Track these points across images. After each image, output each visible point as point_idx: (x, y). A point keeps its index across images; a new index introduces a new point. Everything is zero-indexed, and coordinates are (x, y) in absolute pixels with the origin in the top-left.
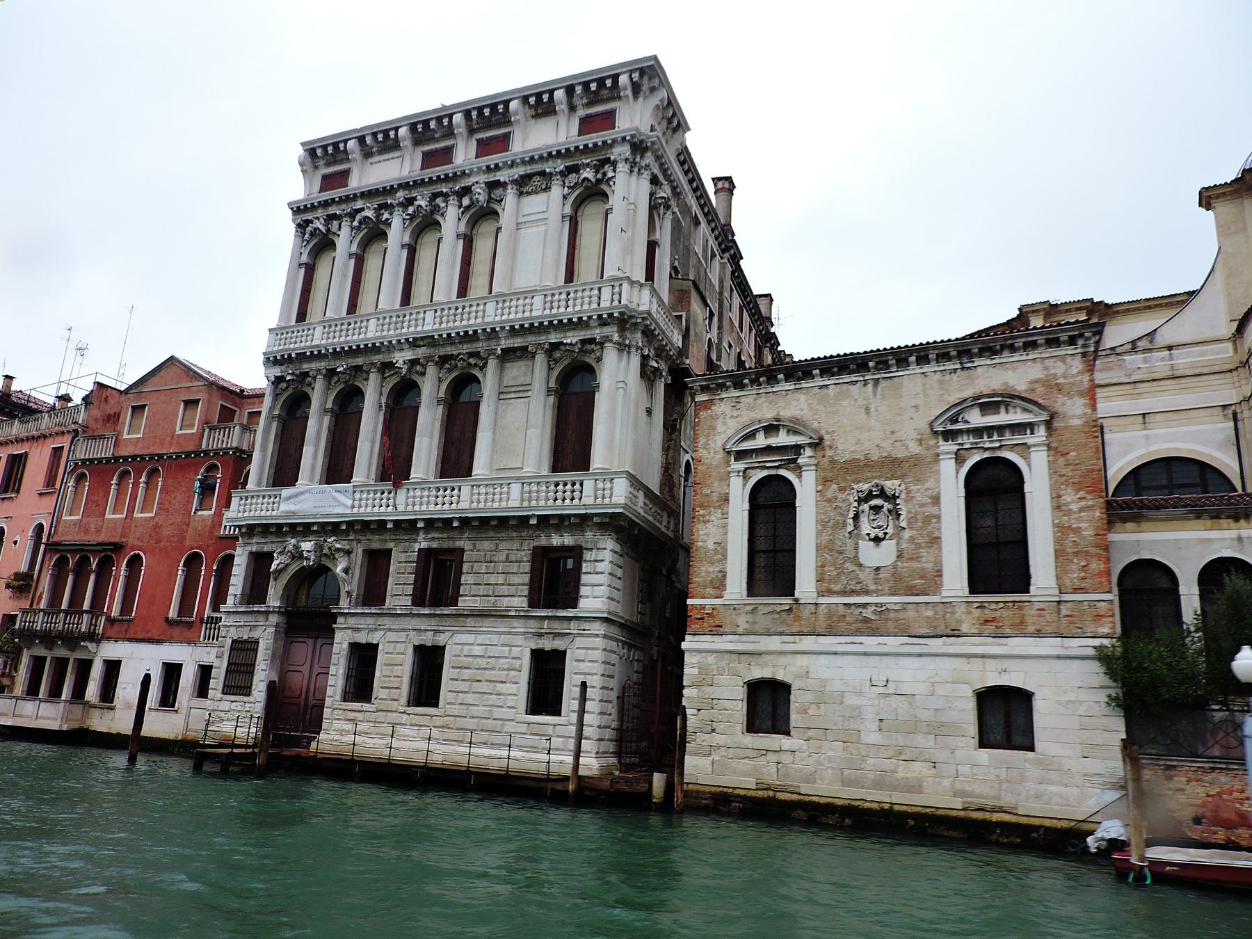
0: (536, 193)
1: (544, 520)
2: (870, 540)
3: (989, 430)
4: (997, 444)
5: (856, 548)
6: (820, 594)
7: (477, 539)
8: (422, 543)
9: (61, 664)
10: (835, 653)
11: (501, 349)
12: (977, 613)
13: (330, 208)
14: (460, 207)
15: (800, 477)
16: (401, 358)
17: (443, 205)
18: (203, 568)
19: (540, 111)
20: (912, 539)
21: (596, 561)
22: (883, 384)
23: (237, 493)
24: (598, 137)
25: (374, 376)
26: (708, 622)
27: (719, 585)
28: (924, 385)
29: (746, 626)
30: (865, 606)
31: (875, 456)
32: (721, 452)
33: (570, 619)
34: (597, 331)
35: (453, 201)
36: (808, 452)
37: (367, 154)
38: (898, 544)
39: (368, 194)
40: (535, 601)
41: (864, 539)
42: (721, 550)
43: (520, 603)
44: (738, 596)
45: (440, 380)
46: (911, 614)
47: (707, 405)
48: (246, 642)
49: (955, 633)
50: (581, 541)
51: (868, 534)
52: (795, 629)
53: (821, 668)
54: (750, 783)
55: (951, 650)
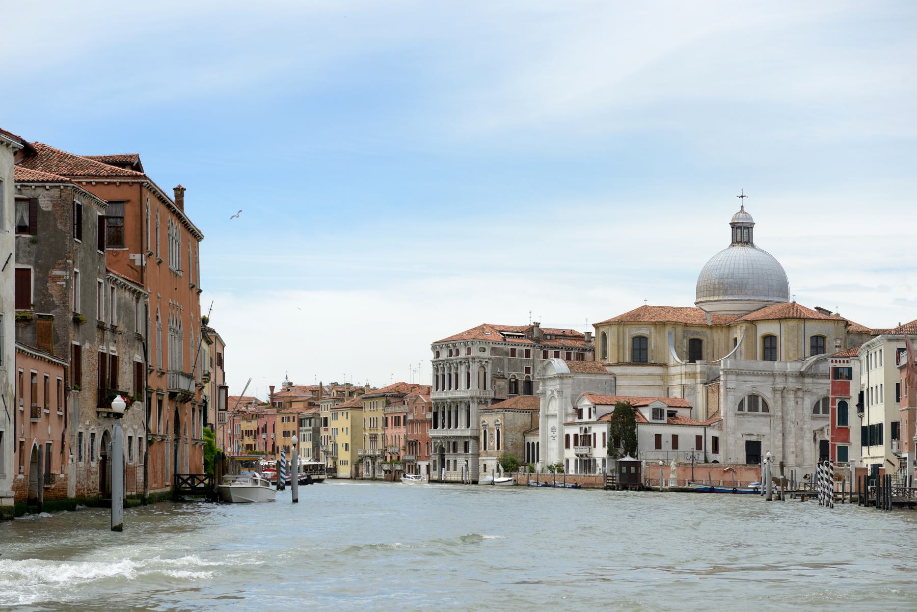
9: (412, 466)
39: (441, 361)
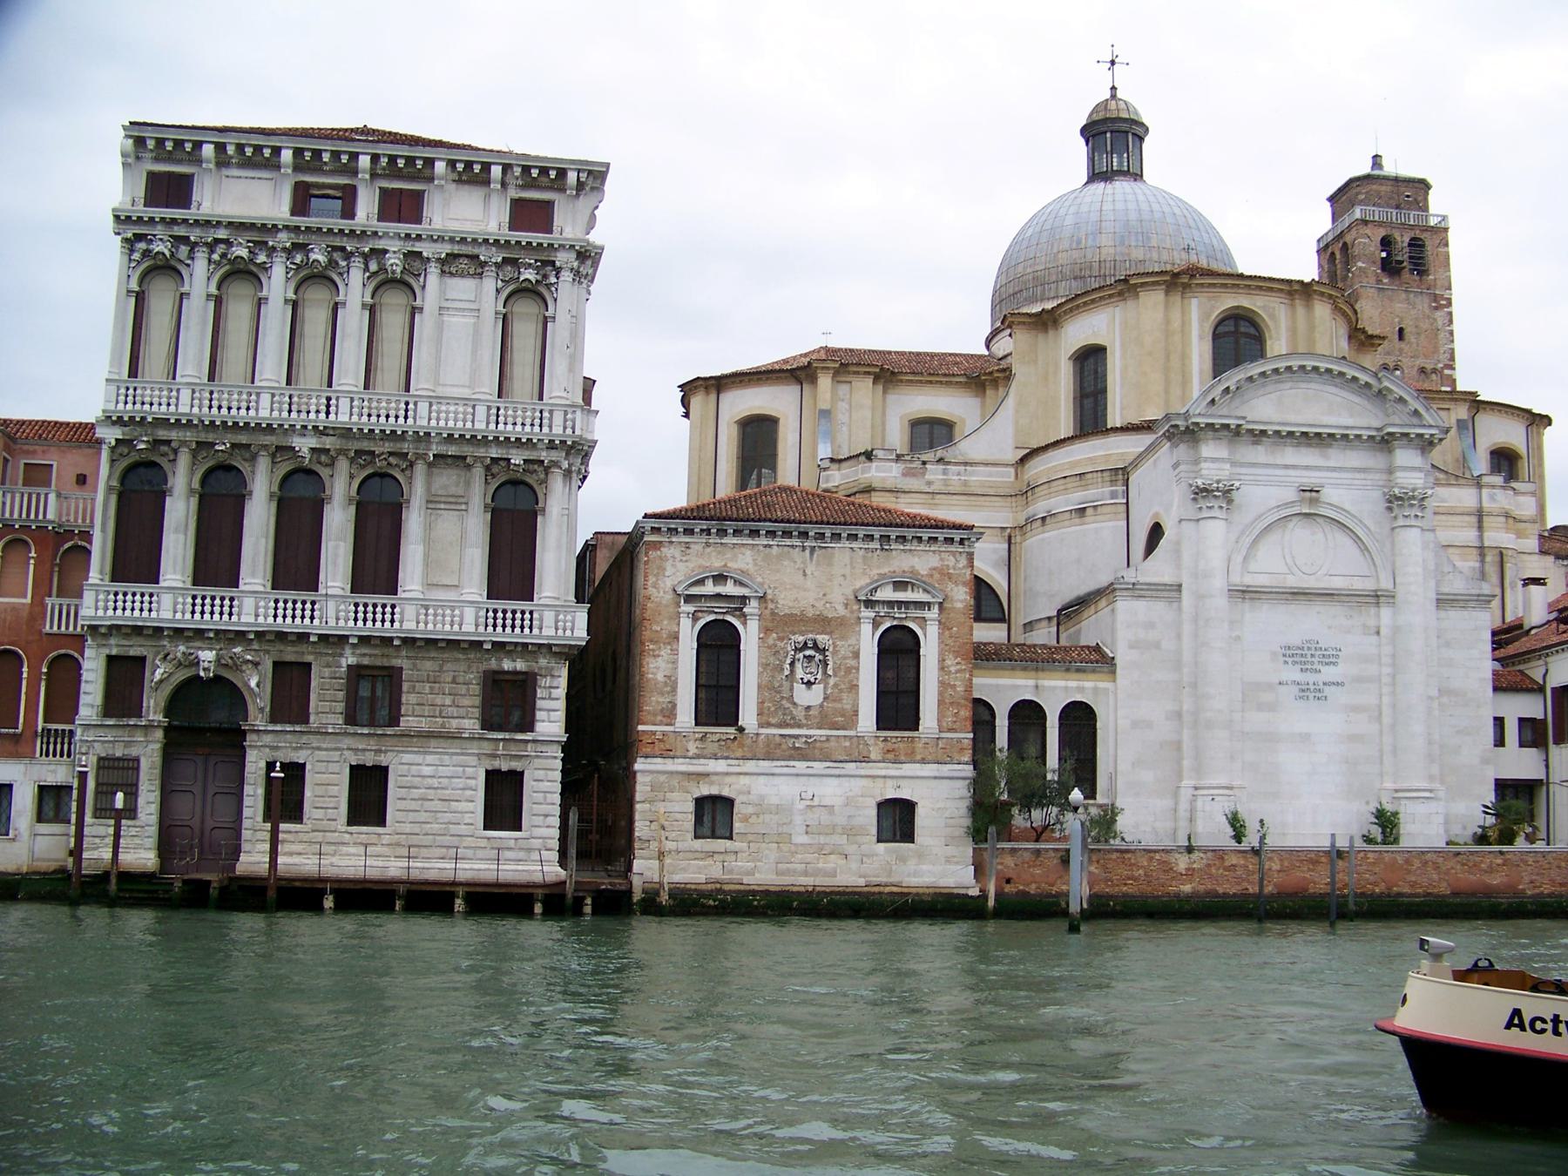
0: (462, 276)
1: (499, 646)
2: (803, 683)
3: (900, 603)
4: (904, 616)
5: (792, 689)
6: (761, 726)
7: (417, 658)
8: (349, 659)
10: (773, 775)
11: (434, 455)
12: (881, 745)
13: (176, 228)
14: (366, 269)
15: (744, 624)
16: (304, 445)
17: (344, 263)
18: (25, 669)
19: (464, 178)
20: (836, 685)
21: (551, 687)
22: (818, 552)
24: (544, 238)
25: (263, 463)
26: (659, 747)
27: (670, 714)
28: (851, 558)
29: (696, 751)
30: (797, 737)
31: (810, 613)
32: (671, 592)
33: (527, 741)
34: (544, 454)
35: (357, 262)
36: (754, 603)
37: (222, 162)
38: (825, 688)
40: (487, 725)
41: (798, 682)
42: (672, 684)
43: (471, 725)
44: (689, 725)
45: (352, 477)
46: (833, 744)
47: (657, 546)
48: (119, 759)
49: (866, 760)
50: (535, 667)
51: (802, 679)
52: (738, 754)
53: (761, 787)
54: (701, 878)
55: (863, 772)
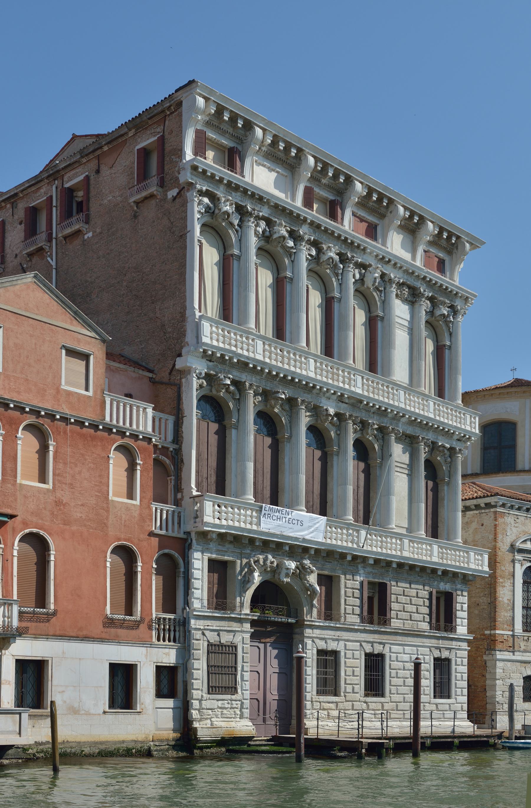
23: (211, 497)
